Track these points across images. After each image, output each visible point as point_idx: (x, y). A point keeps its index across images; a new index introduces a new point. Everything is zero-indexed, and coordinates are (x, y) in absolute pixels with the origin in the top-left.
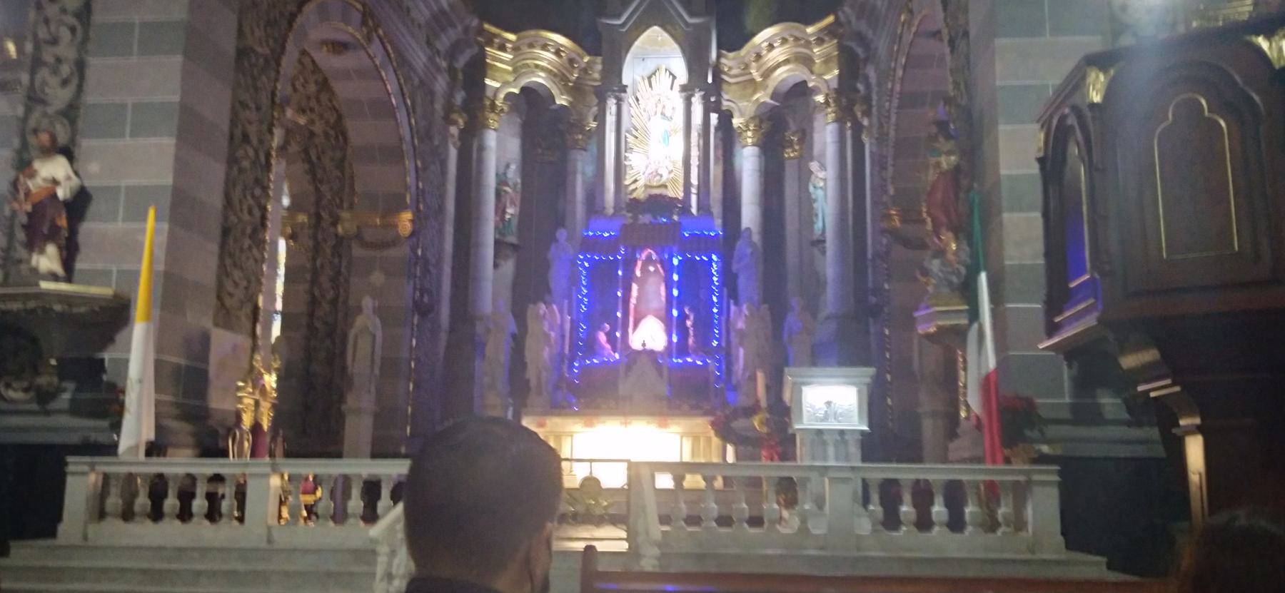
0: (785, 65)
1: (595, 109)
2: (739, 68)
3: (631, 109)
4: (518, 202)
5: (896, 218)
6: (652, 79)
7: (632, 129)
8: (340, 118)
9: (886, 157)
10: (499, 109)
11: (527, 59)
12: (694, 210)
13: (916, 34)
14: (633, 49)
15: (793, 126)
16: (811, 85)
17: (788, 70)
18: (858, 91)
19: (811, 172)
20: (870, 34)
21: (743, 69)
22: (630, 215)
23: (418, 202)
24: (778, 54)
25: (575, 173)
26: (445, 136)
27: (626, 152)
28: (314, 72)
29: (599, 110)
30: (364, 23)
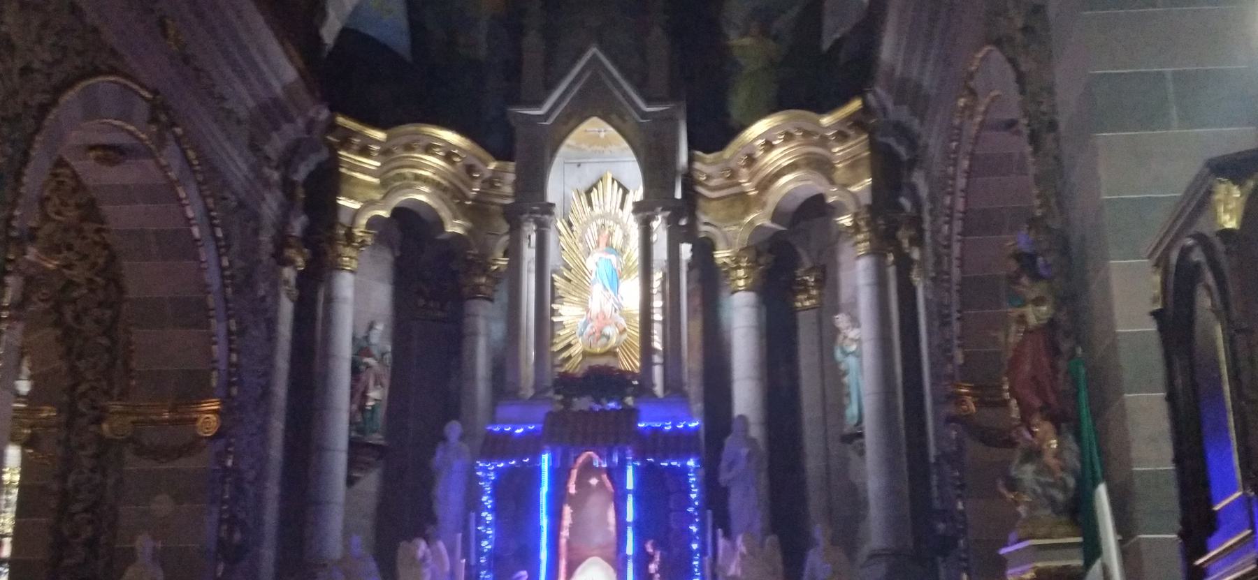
0: (789, 173)
1: (505, 239)
2: (722, 176)
3: (562, 238)
4: (386, 381)
5: (969, 399)
6: (592, 194)
7: (562, 268)
8: (112, 258)
9: (948, 306)
10: (360, 240)
11: (402, 167)
12: (658, 389)
13: (982, 125)
14: (563, 150)
15: (807, 262)
16: (831, 200)
17: (796, 180)
18: (901, 208)
19: (836, 331)
20: (915, 124)
21: (728, 178)
22: (560, 397)
23: (230, 384)
24: (778, 157)
25: (475, 334)
26: (275, 284)
27: (553, 302)
28: (74, 191)
29: (511, 240)
30: (154, 120)
